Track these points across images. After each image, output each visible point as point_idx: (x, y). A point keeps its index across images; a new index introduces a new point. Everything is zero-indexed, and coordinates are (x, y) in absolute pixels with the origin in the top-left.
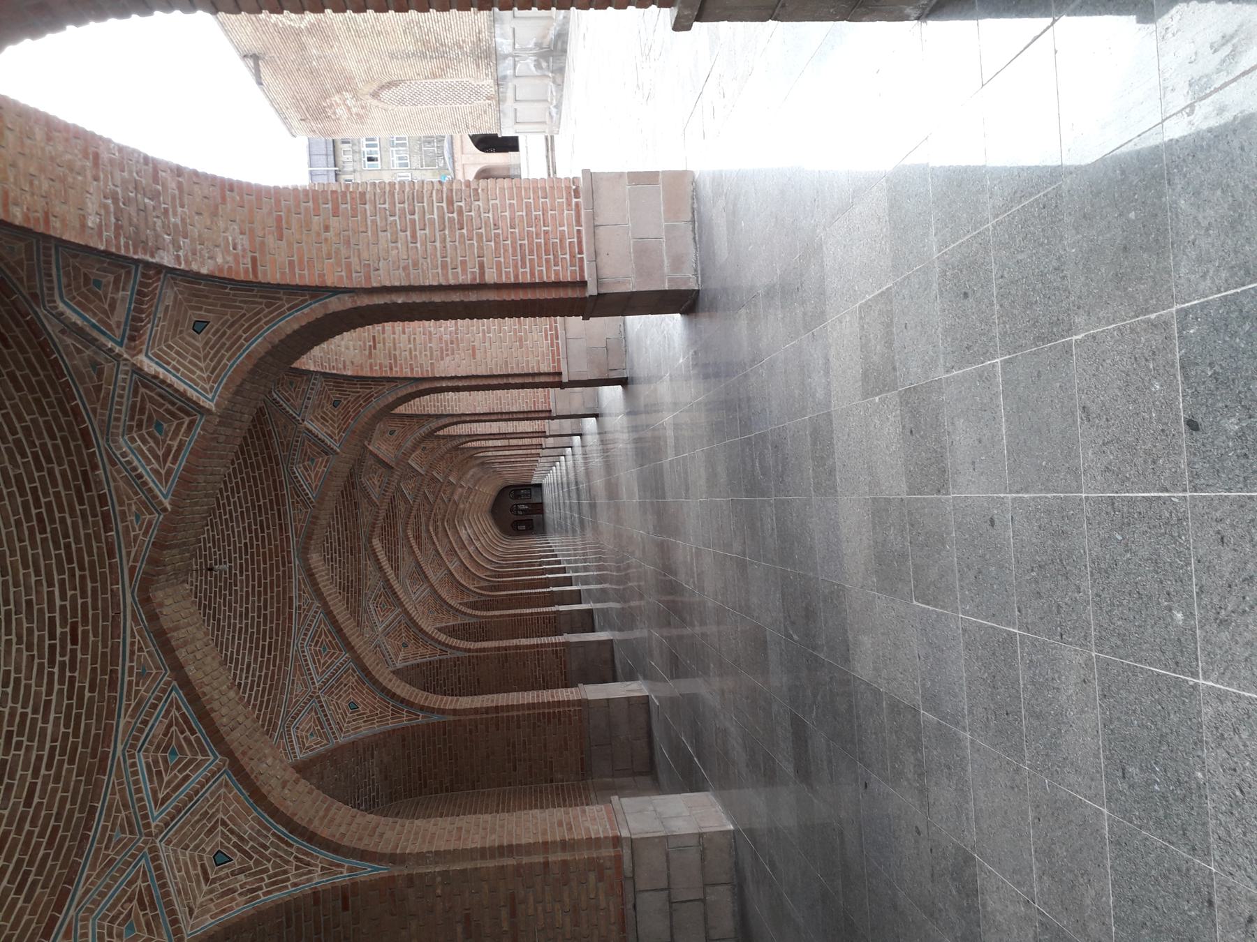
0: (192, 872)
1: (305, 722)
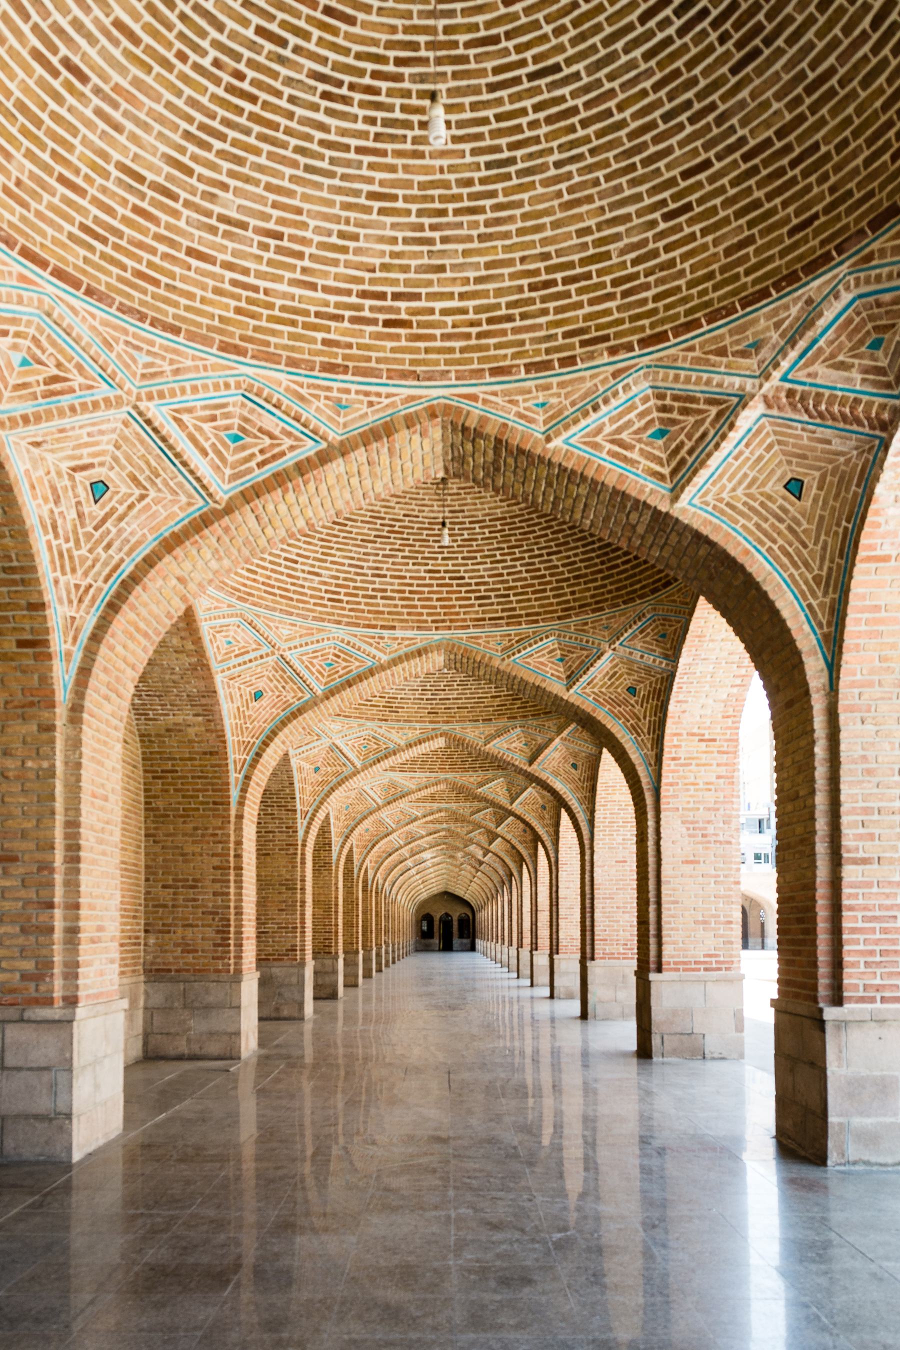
0: (85, 451)
1: (245, 636)
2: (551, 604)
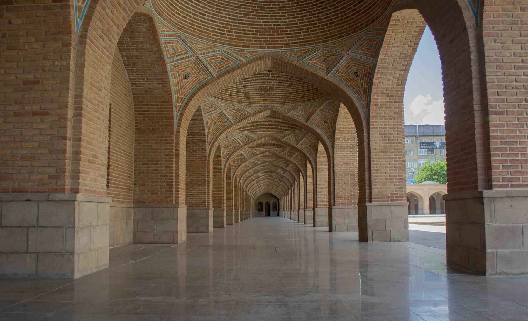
1: (181, 46)
2: (319, 36)
